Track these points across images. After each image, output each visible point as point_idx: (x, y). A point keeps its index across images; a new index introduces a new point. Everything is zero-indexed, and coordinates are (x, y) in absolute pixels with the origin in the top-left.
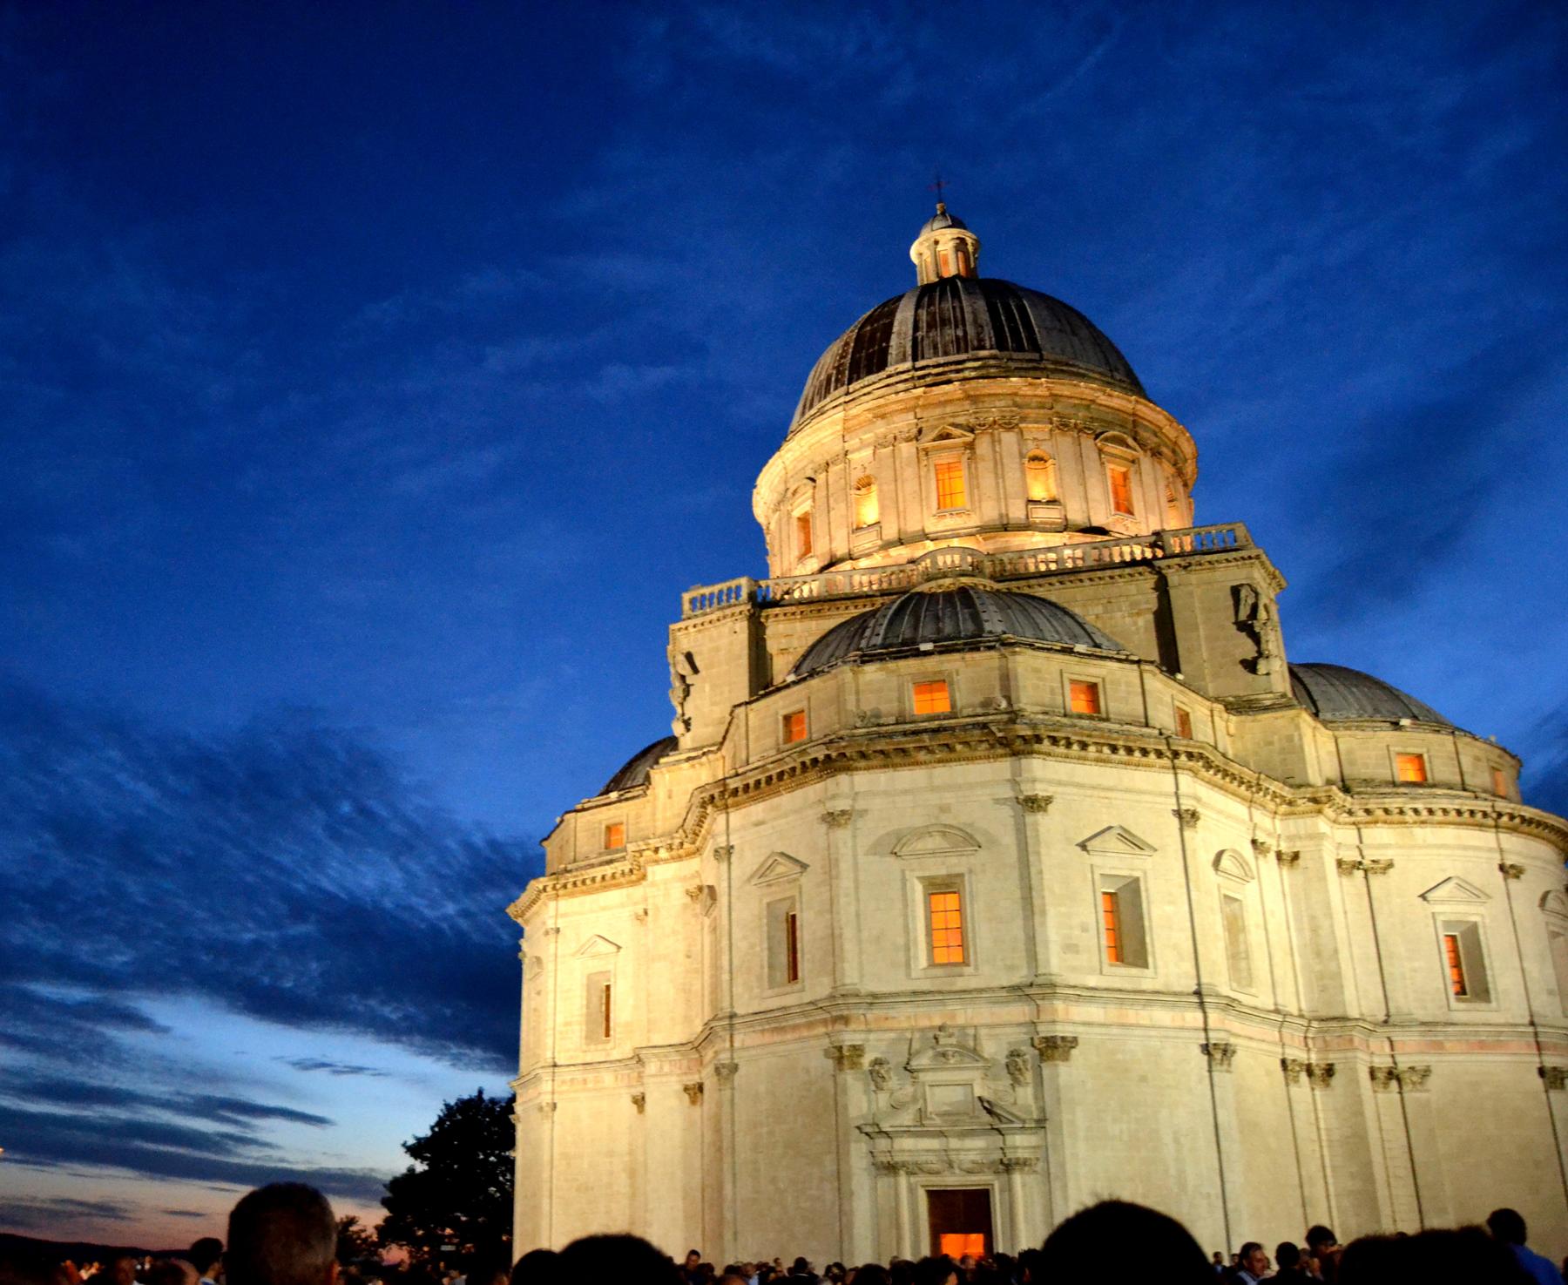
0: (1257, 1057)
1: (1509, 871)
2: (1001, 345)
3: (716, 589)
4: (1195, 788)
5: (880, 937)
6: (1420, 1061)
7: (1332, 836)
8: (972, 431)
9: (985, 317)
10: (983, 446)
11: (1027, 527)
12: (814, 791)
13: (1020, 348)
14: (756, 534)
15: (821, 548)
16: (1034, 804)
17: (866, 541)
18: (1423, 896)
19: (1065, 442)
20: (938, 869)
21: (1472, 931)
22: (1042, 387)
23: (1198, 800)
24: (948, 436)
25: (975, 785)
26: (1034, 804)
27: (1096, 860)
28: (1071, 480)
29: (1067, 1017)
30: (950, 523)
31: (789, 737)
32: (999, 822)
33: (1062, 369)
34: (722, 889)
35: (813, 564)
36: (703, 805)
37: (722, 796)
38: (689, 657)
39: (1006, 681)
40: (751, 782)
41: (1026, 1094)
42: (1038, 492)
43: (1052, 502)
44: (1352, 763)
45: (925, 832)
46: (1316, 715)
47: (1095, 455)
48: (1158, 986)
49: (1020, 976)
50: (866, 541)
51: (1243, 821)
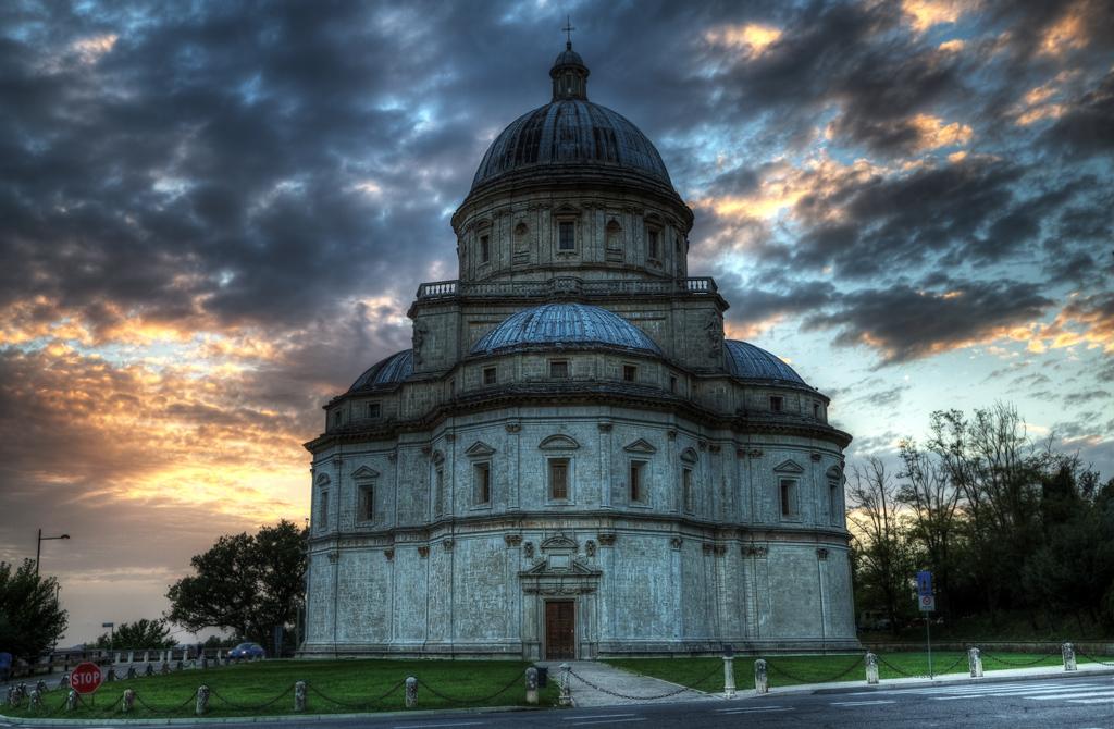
1: (816, 458)
2: (598, 158)
9: (592, 139)
10: (586, 218)
13: (610, 159)
18: (775, 469)
19: (628, 219)
20: (558, 455)
23: (677, 426)
24: (569, 209)
27: (631, 455)
28: (628, 238)
31: (488, 381)
36: (441, 412)
40: (469, 404)
43: (618, 251)
44: (749, 400)
47: (642, 226)
48: (653, 512)
51: (695, 433)
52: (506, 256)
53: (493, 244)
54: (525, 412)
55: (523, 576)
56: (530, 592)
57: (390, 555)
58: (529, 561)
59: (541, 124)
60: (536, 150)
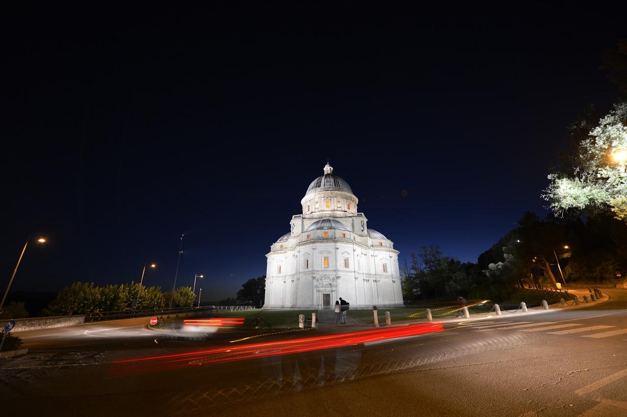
0: (360, 279)
1: (391, 257)
4: (356, 247)
5: (318, 264)
6: (379, 279)
7: (371, 252)
9: (333, 182)
10: (332, 199)
11: (337, 210)
12: (311, 245)
14: (301, 206)
15: (310, 210)
16: (337, 249)
17: (317, 210)
21: (386, 264)
25: (330, 246)
26: (337, 249)
28: (343, 205)
29: (340, 274)
30: (328, 209)
32: (333, 251)
33: (342, 190)
34: (298, 256)
35: (310, 212)
37: (300, 244)
39: (335, 233)
41: (335, 283)
42: (339, 206)
45: (324, 251)
46: (370, 237)
52: (314, 209)
53: (310, 207)
54: (317, 244)
55: (317, 287)
56: (319, 291)
57: (285, 282)
58: (318, 283)
60: (320, 185)
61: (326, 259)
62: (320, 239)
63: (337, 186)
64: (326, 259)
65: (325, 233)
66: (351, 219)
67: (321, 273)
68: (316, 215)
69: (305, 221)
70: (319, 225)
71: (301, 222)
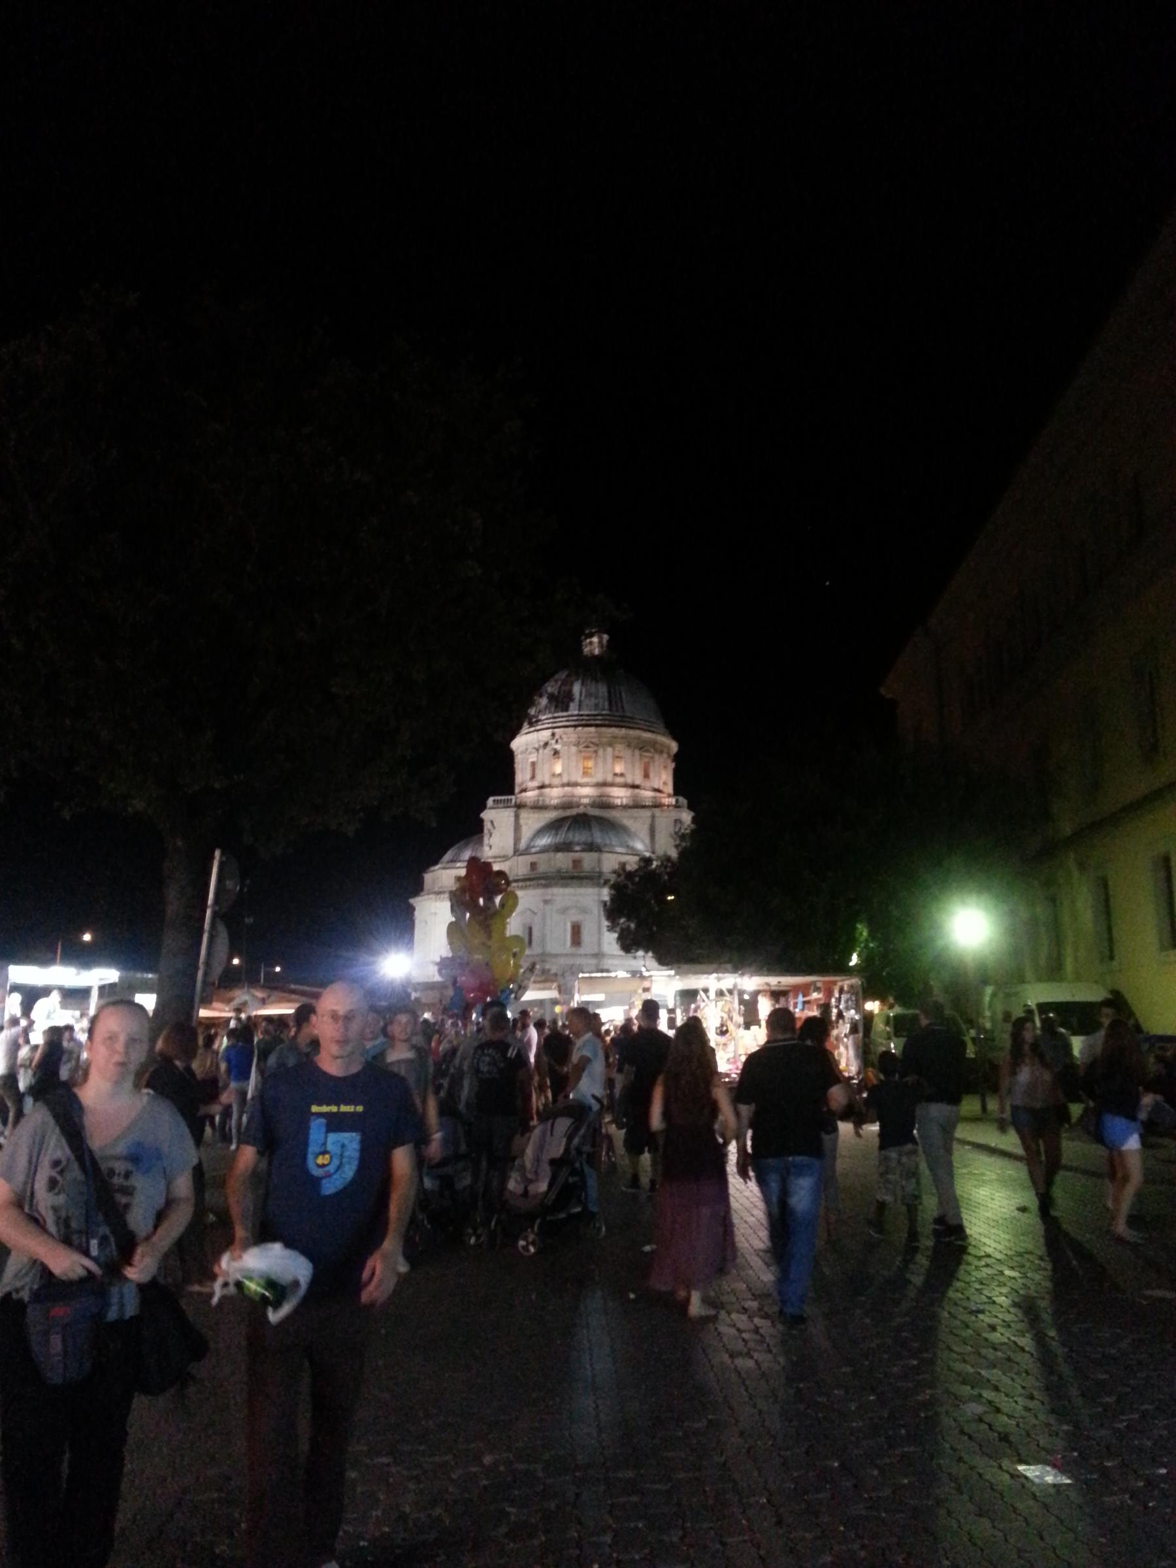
2: (610, 710)
3: (503, 798)
8: (597, 745)
10: (601, 752)
11: (612, 785)
12: (539, 891)
14: (510, 756)
17: (556, 781)
20: (574, 919)
22: (623, 731)
30: (586, 780)
35: (535, 784)
38: (492, 822)
39: (599, 861)
42: (618, 769)
43: (622, 775)
49: (596, 951)
50: (556, 781)
54: (556, 890)
59: (572, 685)
61: (576, 930)
62: (563, 878)
63: (614, 717)
64: (576, 930)
65: (574, 861)
66: (647, 813)
67: (562, 961)
68: (555, 795)
69: (524, 814)
70: (560, 838)
71: (512, 819)
